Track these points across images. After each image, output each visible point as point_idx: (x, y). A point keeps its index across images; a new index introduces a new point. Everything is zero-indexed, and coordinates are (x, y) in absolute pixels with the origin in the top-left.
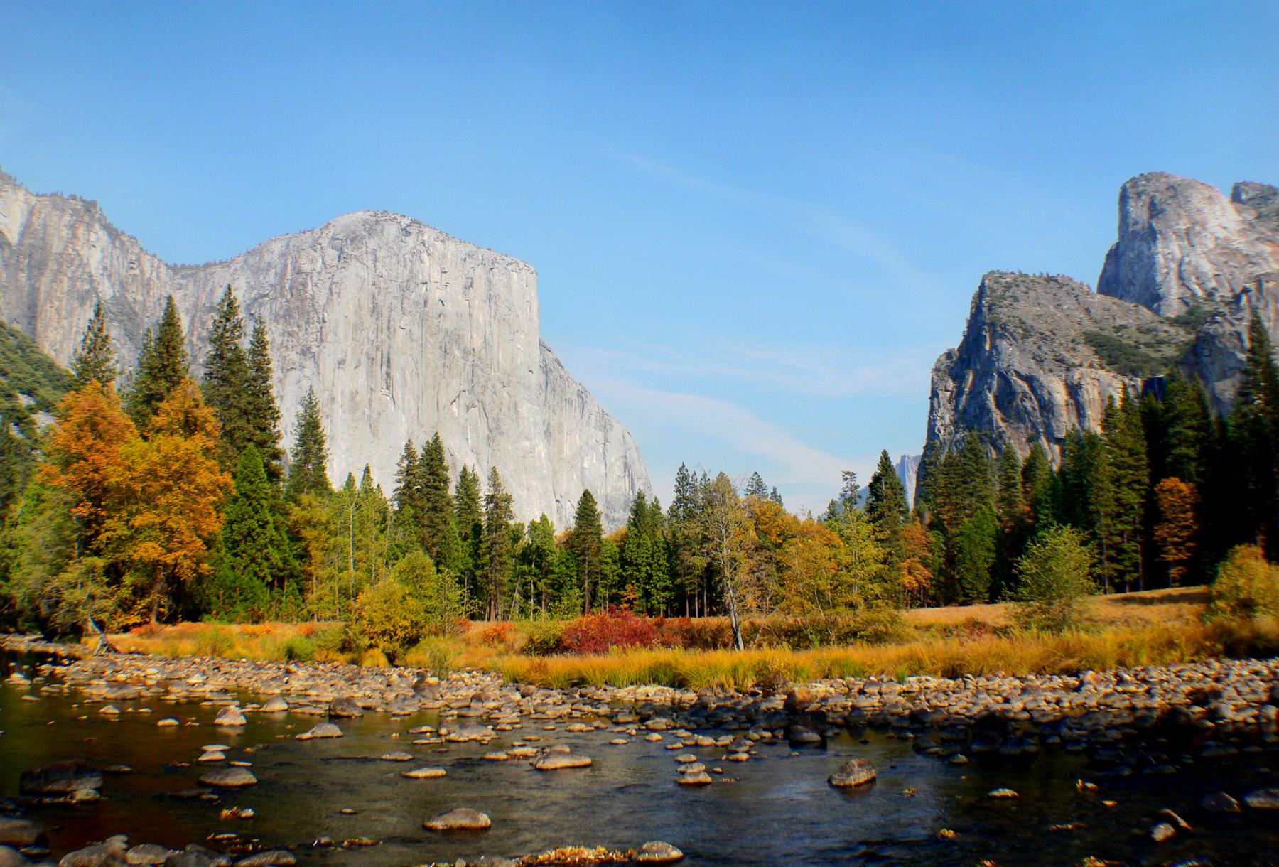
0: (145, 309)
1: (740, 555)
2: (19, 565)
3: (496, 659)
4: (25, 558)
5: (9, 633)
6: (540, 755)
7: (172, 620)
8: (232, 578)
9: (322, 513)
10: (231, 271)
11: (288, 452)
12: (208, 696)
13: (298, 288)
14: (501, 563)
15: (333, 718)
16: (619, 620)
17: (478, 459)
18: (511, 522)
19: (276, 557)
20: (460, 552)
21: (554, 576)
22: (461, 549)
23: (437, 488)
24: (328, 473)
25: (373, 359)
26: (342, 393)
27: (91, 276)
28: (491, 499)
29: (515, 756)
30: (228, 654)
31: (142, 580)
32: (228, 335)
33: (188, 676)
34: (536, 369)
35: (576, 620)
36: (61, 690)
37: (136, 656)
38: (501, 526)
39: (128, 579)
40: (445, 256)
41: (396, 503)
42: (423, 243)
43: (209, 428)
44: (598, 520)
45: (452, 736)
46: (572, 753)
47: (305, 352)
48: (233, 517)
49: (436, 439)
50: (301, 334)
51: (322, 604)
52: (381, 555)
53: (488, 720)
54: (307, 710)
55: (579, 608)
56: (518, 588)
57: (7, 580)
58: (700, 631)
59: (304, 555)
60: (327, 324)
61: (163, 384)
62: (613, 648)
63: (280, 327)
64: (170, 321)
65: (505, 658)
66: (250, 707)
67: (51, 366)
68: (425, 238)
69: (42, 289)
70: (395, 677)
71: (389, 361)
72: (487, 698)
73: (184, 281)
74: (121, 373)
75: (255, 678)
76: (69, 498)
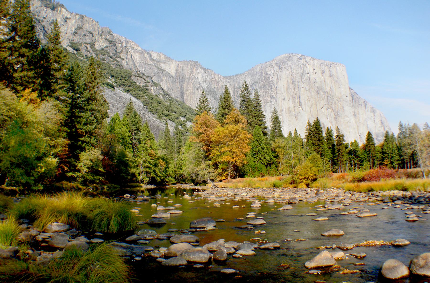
0: (218, 89)
1: (423, 148)
2: (185, 165)
3: (342, 184)
4: (187, 163)
5: (183, 184)
6: (359, 213)
7: (235, 177)
8: (254, 165)
9: (282, 143)
10: (244, 76)
11: (269, 127)
12: (248, 199)
13: (267, 78)
14: (342, 155)
15: (290, 203)
16: (383, 170)
17: (332, 124)
18: (345, 143)
19: (268, 158)
20: (329, 153)
21: (360, 158)
22: (328, 152)
23: (319, 134)
24: (283, 132)
25: (294, 97)
26: (285, 108)
27: (199, 82)
28: (337, 136)
29: (351, 213)
30: (254, 186)
31: (225, 167)
32: (246, 94)
33: (241, 193)
34: (349, 96)
35: (368, 171)
36: (201, 199)
37: (224, 188)
38: (341, 144)
39: (220, 167)
40: (314, 65)
41: (306, 139)
42: (306, 61)
43: (243, 121)
44: (373, 140)
45: (330, 208)
46: (370, 212)
47: (272, 97)
48: (253, 147)
49: (318, 119)
50: (269, 92)
51: (284, 170)
52: (302, 155)
53: (341, 202)
54: (281, 202)
55: (369, 168)
56: (348, 162)
57: (181, 169)
58: (411, 173)
59: (277, 157)
60: (278, 89)
61: (227, 111)
62: (382, 179)
63: (262, 91)
64: (227, 92)
65: (345, 184)
66: (262, 201)
67: (190, 108)
68: (307, 60)
69: (184, 87)
70: (309, 191)
71: (299, 97)
72: (340, 196)
73: (230, 81)
74: (213, 108)
75: (263, 193)
76: (200, 145)
